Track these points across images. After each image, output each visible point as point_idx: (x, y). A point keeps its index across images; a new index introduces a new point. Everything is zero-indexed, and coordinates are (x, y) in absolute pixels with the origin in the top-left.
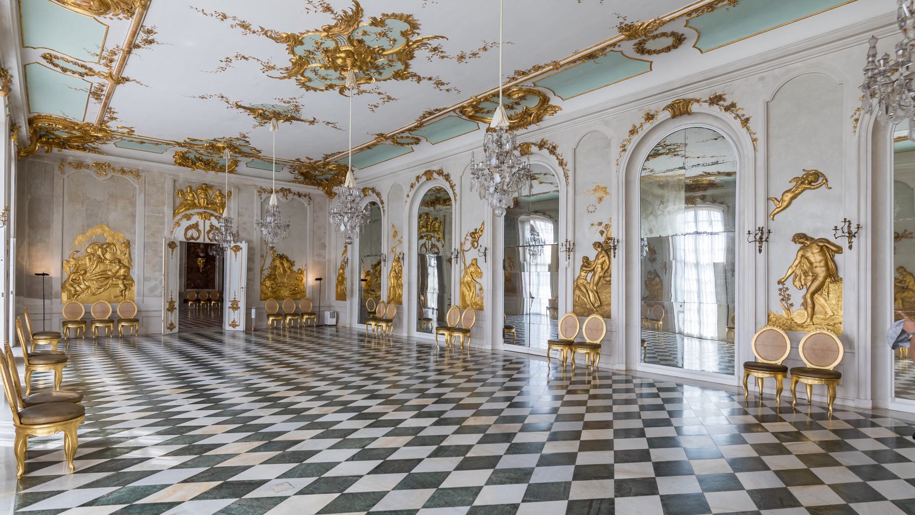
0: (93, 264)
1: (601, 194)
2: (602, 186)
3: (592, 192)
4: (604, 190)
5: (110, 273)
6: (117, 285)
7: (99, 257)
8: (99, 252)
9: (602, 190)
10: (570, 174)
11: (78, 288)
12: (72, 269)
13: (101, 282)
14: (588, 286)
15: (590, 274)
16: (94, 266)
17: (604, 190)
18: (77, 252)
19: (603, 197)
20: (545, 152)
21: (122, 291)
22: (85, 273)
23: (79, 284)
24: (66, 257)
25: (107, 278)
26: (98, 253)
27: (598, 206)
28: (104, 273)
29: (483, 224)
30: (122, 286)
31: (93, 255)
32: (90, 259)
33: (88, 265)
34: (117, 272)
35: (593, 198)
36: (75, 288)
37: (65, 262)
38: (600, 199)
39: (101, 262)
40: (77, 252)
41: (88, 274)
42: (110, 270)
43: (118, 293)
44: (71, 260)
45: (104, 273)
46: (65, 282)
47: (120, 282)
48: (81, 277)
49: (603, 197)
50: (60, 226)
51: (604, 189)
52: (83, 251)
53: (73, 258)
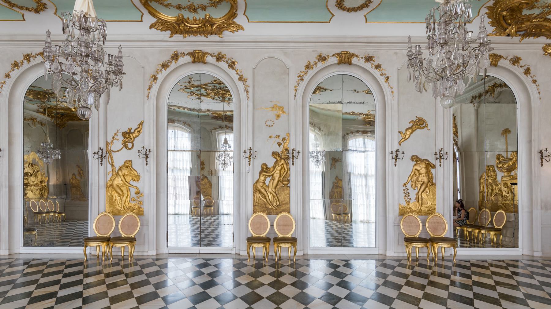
1: (279, 112)
2: (279, 105)
3: (270, 109)
4: (281, 109)
9: (279, 109)
10: (250, 90)
14: (267, 189)
15: (268, 179)
17: (281, 109)
19: (280, 115)
20: (223, 65)
27: (276, 121)
29: (141, 124)
35: (271, 115)
38: (278, 116)
49: (280, 115)
51: (282, 109)
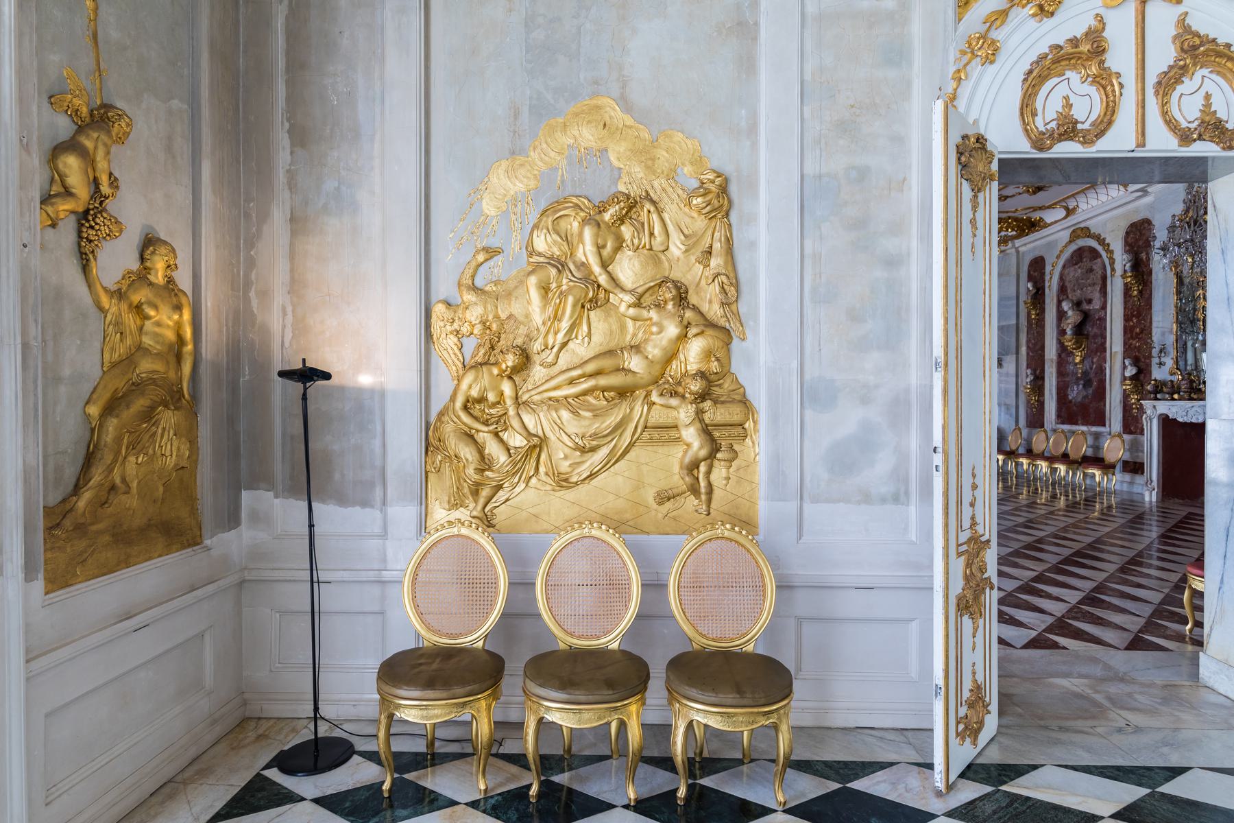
0: (557, 318)
5: (635, 363)
6: (666, 432)
7: (588, 279)
8: (586, 252)
11: (493, 449)
12: (470, 344)
13: (597, 414)
16: (565, 324)
18: (491, 252)
21: (693, 466)
22: (526, 359)
23: (498, 426)
24: (444, 287)
25: (623, 393)
26: (580, 255)
28: (607, 363)
30: (691, 435)
31: (561, 266)
32: (545, 289)
33: (538, 317)
34: (671, 356)
36: (480, 450)
37: (439, 309)
39: (594, 303)
40: (491, 252)
41: (538, 372)
42: (636, 348)
43: (678, 480)
44: (469, 297)
45: (607, 363)
46: (441, 414)
47: (685, 413)
48: (507, 388)
50: (412, 117)
52: (515, 246)
53: (474, 288)
